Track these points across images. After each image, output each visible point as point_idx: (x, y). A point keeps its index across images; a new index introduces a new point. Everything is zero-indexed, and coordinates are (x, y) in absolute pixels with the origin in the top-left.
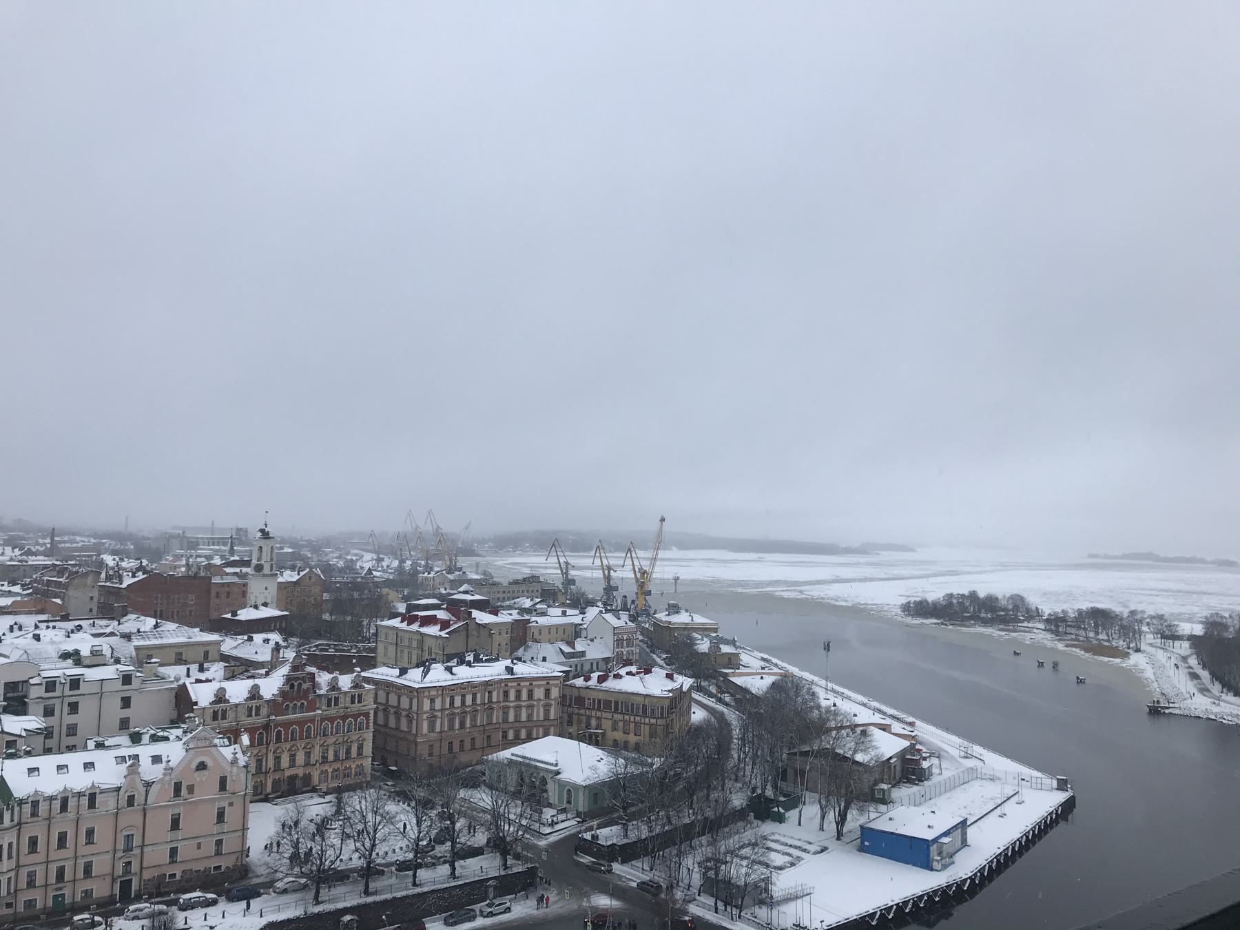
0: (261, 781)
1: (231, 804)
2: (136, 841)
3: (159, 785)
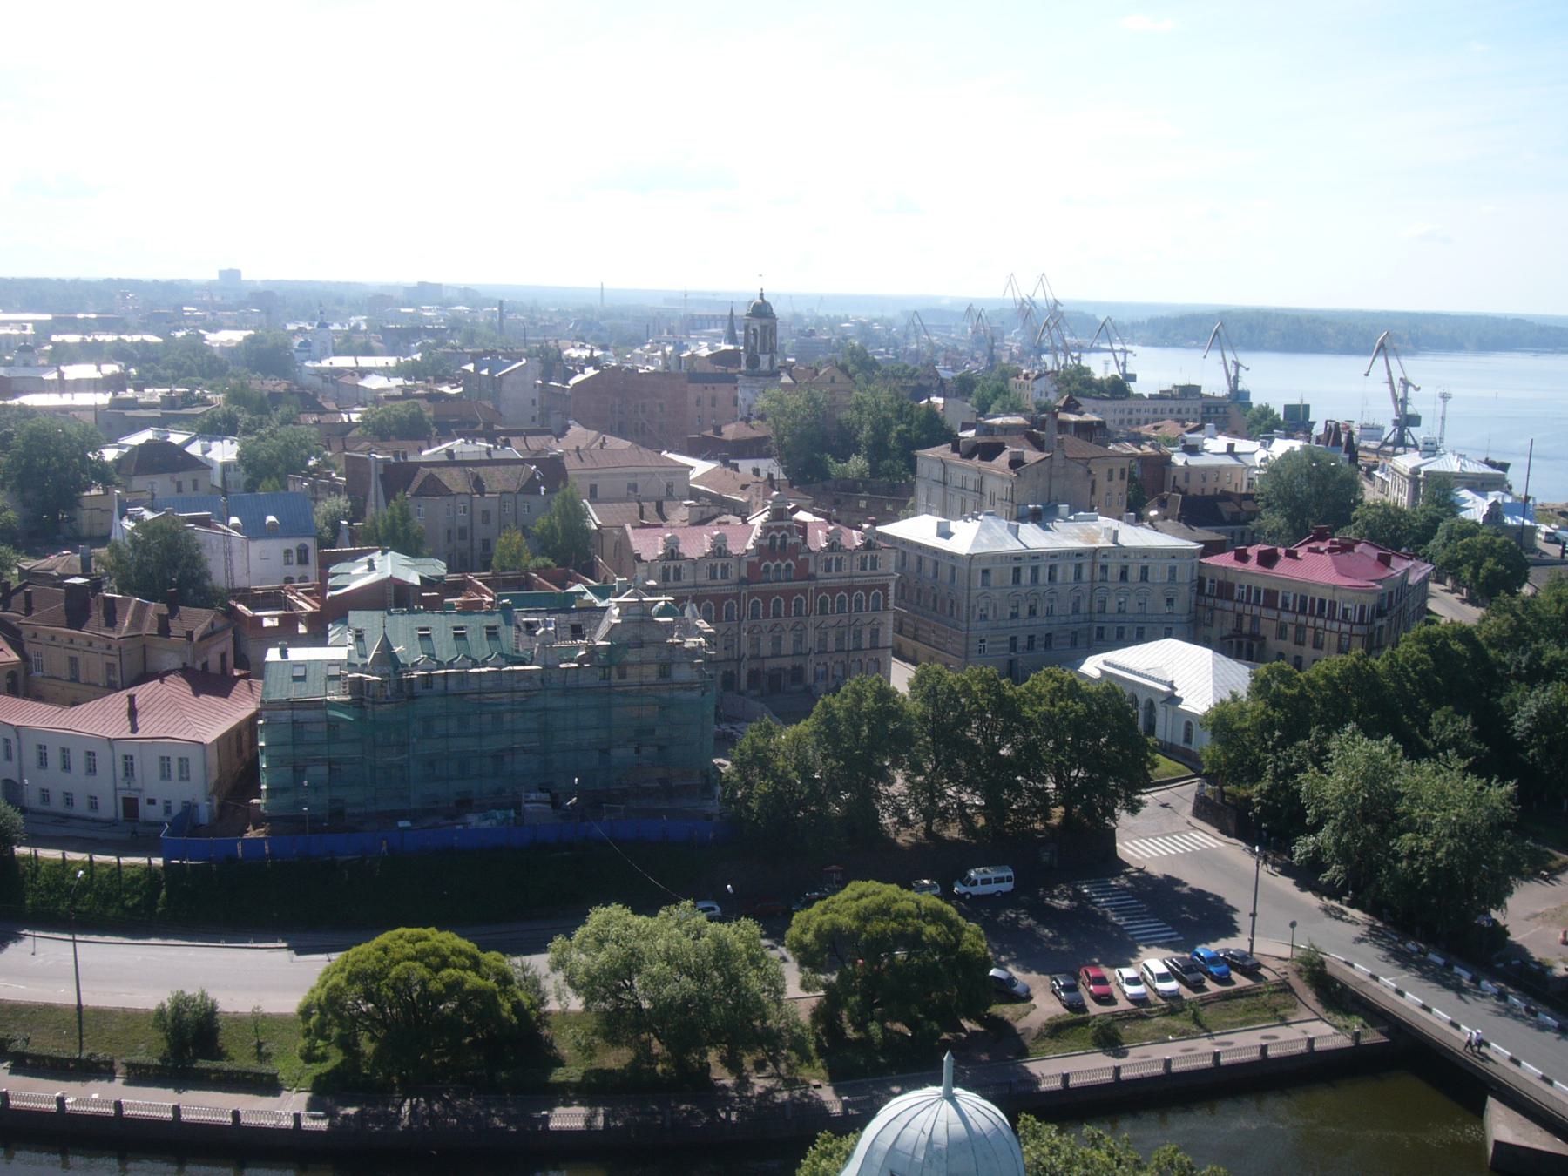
0: (732, 672)
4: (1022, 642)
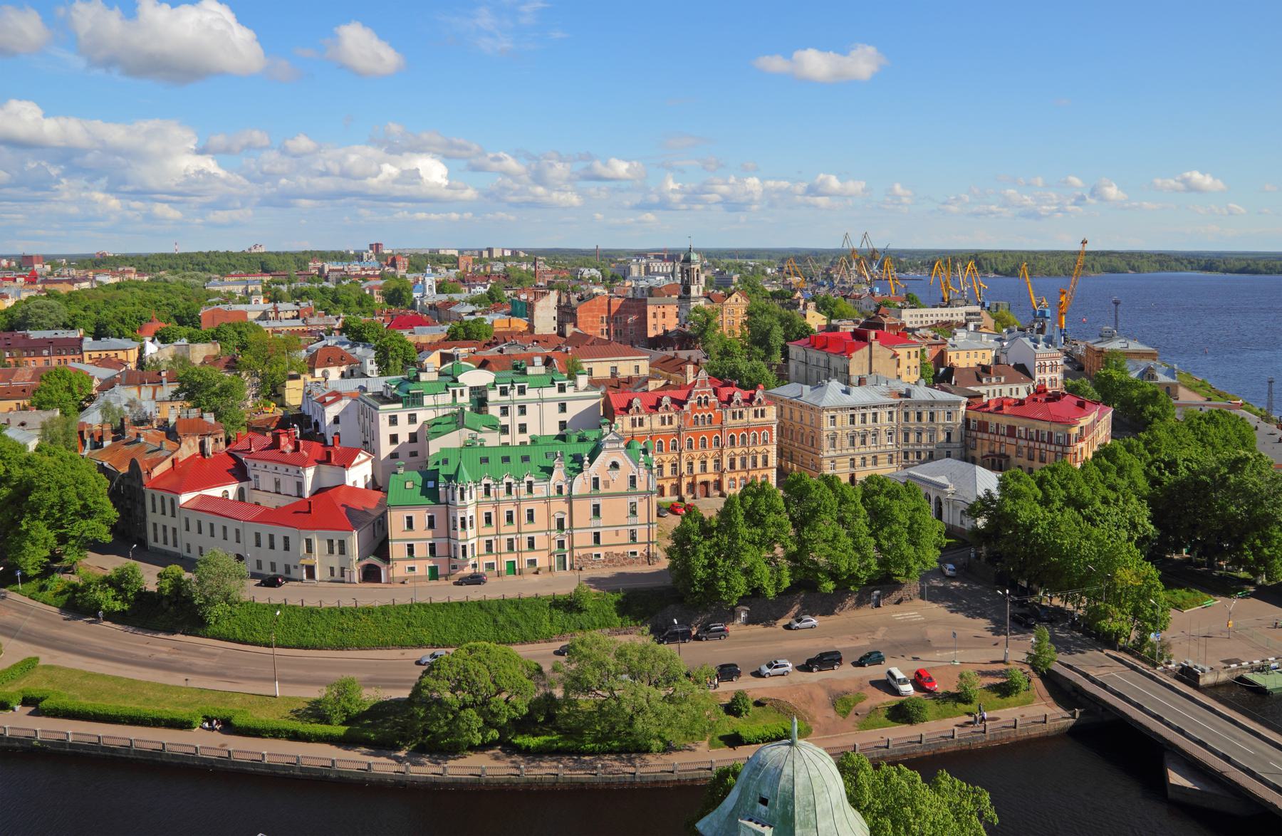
2: (566, 525)
4: (858, 461)
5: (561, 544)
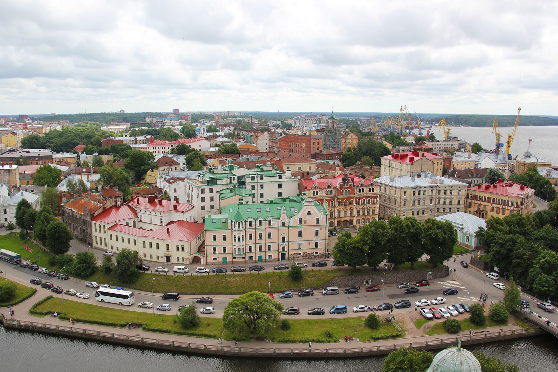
0: (333, 221)
1: (321, 229)
2: (286, 240)
3: (294, 219)
4: (416, 213)
5: (283, 248)
